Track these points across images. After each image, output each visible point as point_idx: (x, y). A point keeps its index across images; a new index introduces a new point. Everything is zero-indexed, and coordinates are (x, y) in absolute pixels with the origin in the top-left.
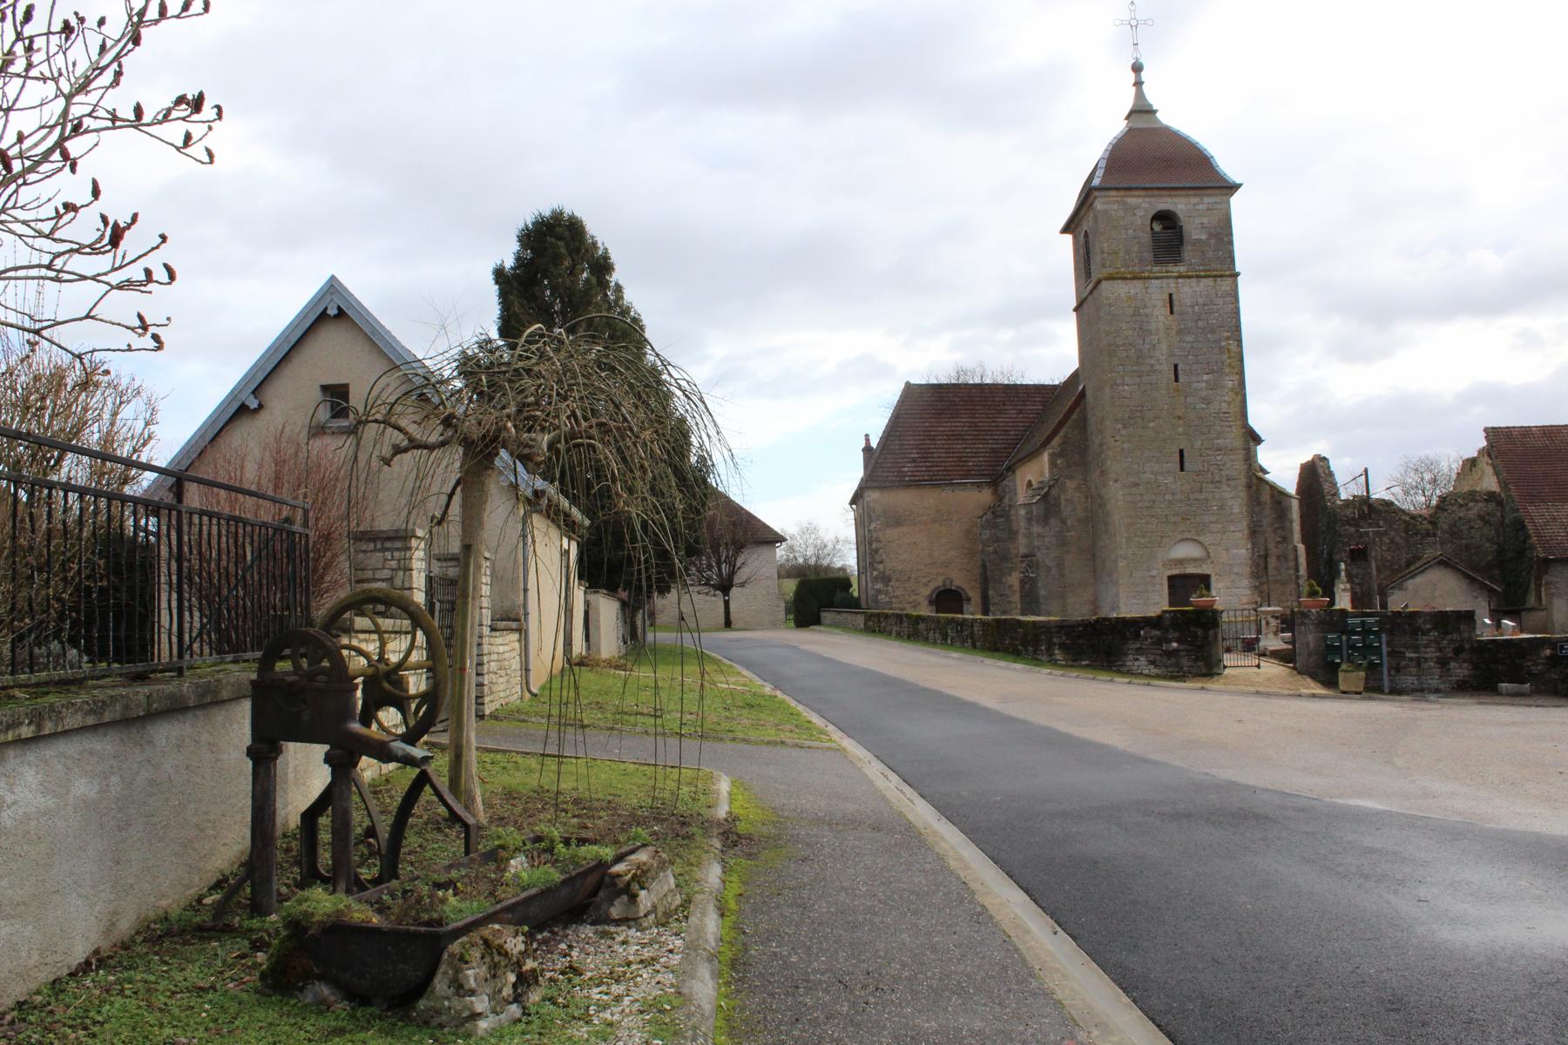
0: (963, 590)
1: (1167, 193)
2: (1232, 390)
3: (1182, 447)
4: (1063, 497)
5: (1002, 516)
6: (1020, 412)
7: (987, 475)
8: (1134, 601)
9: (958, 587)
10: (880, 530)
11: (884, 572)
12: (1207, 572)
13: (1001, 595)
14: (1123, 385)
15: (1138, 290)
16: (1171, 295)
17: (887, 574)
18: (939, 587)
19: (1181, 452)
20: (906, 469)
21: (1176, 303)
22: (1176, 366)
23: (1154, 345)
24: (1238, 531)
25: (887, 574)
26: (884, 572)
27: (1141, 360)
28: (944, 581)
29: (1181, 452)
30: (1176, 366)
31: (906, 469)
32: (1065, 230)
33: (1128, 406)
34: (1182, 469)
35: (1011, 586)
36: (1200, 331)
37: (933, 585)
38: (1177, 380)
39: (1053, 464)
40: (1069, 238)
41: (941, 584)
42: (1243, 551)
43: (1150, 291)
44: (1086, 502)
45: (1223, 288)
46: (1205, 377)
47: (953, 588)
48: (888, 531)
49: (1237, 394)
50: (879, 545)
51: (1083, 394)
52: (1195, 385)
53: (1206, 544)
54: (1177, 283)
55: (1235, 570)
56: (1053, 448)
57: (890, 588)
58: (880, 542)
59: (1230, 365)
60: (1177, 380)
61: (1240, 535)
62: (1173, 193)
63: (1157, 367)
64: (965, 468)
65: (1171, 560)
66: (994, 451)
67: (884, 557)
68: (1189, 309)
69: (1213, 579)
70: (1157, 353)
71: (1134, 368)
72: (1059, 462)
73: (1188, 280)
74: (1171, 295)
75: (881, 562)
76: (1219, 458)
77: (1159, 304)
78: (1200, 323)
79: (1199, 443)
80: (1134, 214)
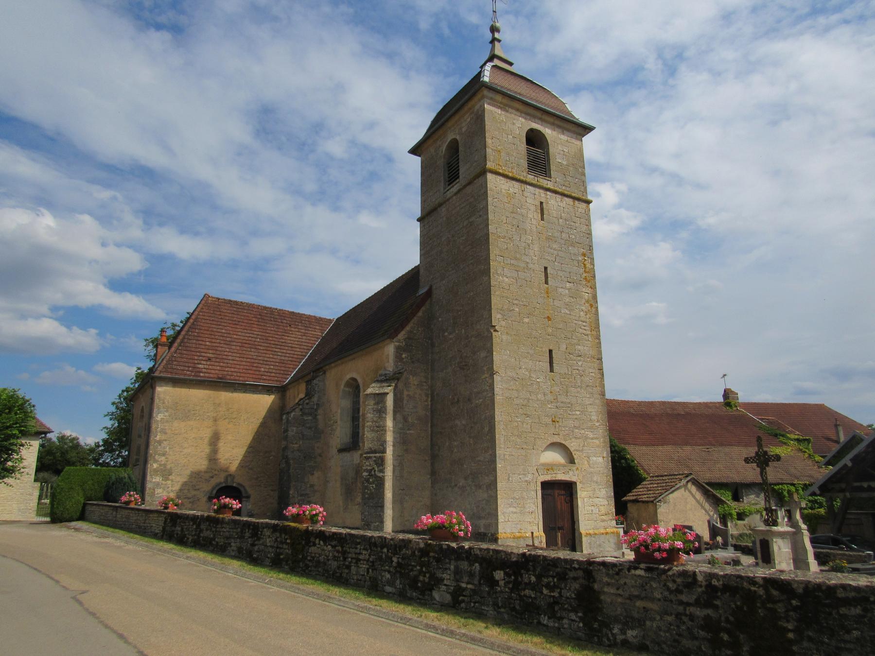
0: (241, 485)
1: (539, 114)
2: (587, 301)
3: (551, 348)
4: (406, 393)
5: (310, 414)
6: (304, 335)
7: (277, 381)
8: (512, 509)
9: (239, 484)
10: (167, 421)
11: (165, 465)
12: (574, 479)
13: (302, 495)
14: (503, 275)
15: (516, 191)
16: (541, 203)
17: (168, 467)
18: (221, 483)
19: (550, 351)
20: (200, 366)
21: (545, 212)
22: (546, 268)
23: (529, 246)
24: (596, 438)
25: (168, 467)
26: (165, 465)
27: (518, 256)
28: (227, 478)
29: (550, 351)
30: (546, 268)
31: (200, 366)
32: (414, 151)
33: (507, 298)
34: (552, 370)
35: (312, 486)
36: (563, 242)
37: (214, 482)
38: (546, 282)
39: (398, 357)
40: (417, 161)
41: (222, 480)
42: (600, 459)
43: (526, 194)
44: (426, 401)
45: (580, 210)
46: (568, 285)
47: (234, 485)
48: (176, 424)
49: (591, 306)
50: (164, 437)
51: (429, 293)
52: (560, 290)
53: (572, 449)
54: (546, 195)
55: (595, 479)
56: (399, 341)
57: (169, 482)
58: (166, 433)
59: (585, 279)
60: (546, 282)
61: (597, 441)
62: (545, 117)
63: (531, 266)
64: (257, 373)
65: (543, 465)
66: (282, 362)
67: (167, 449)
68: (555, 220)
69: (579, 486)
70: (531, 253)
71: (512, 262)
72: (404, 356)
73: (554, 195)
74: (541, 203)
75: (164, 455)
76: (580, 363)
77: (533, 208)
78: (564, 235)
79: (565, 347)
80: (514, 124)
